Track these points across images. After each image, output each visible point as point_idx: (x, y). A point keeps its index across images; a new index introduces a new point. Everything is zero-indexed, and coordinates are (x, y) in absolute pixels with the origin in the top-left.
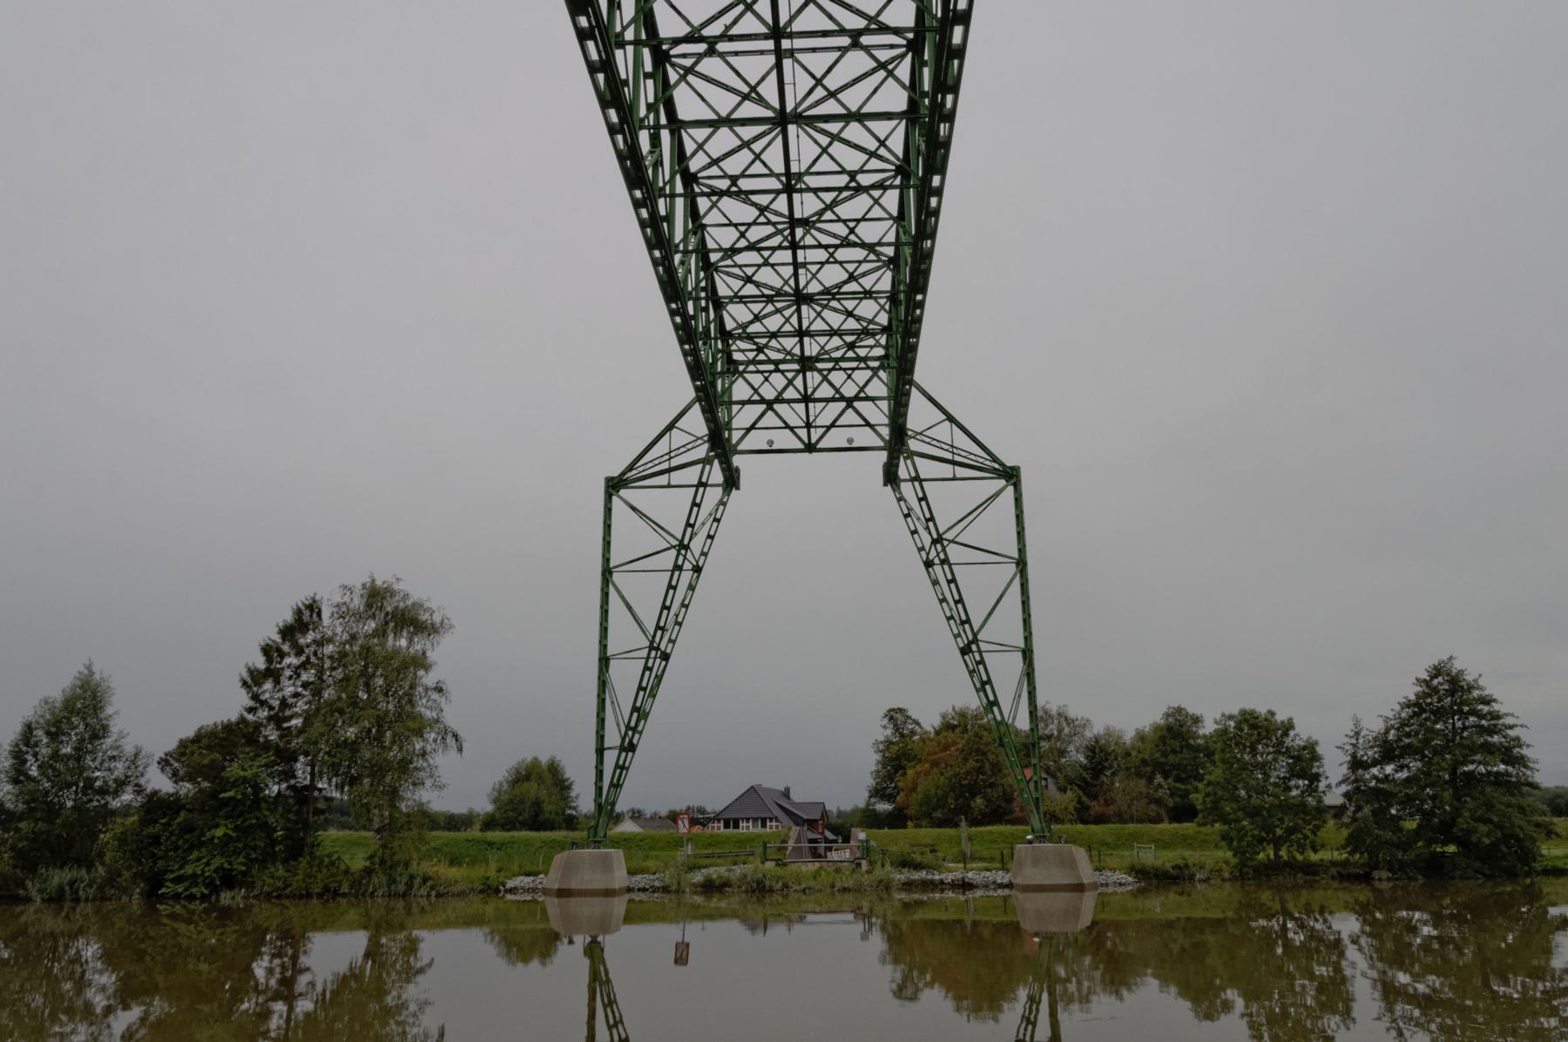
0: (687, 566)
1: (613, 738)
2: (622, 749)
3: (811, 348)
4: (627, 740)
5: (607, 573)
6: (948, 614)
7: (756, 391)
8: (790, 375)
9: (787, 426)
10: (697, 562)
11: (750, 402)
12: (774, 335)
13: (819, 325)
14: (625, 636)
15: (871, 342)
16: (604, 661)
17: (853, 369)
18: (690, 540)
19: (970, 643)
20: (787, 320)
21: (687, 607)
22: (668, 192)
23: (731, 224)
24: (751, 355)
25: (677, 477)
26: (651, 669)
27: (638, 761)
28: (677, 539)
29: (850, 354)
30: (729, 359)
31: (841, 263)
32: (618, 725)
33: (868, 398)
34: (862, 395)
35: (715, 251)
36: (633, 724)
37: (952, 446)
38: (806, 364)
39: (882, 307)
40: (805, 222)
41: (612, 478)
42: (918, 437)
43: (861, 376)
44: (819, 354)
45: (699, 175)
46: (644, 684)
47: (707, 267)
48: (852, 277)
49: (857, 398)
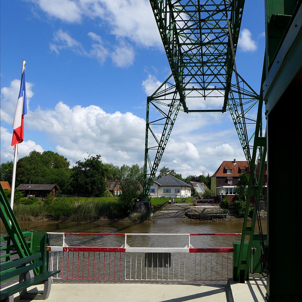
0: (170, 123)
2: (151, 174)
3: (205, 59)
4: (153, 172)
6: (240, 138)
7: (190, 71)
8: (199, 67)
9: (198, 82)
10: (172, 122)
11: (188, 75)
12: (195, 55)
13: (207, 52)
15: (222, 57)
17: (217, 66)
18: (170, 116)
19: (246, 146)
20: (199, 51)
21: (169, 135)
22: (165, 11)
23: (183, 20)
24: (188, 61)
26: (159, 152)
28: (167, 115)
29: (216, 61)
30: (182, 62)
31: (214, 33)
32: (150, 168)
33: (221, 75)
34: (219, 73)
35: (178, 29)
36: (154, 168)
37: (243, 89)
38: (203, 64)
39: (225, 47)
40: (204, 20)
41: (149, 97)
42: (234, 86)
43: (219, 68)
44: (207, 61)
45: (174, 5)
46: (157, 157)
47: (176, 34)
48: (217, 38)
49: (217, 74)
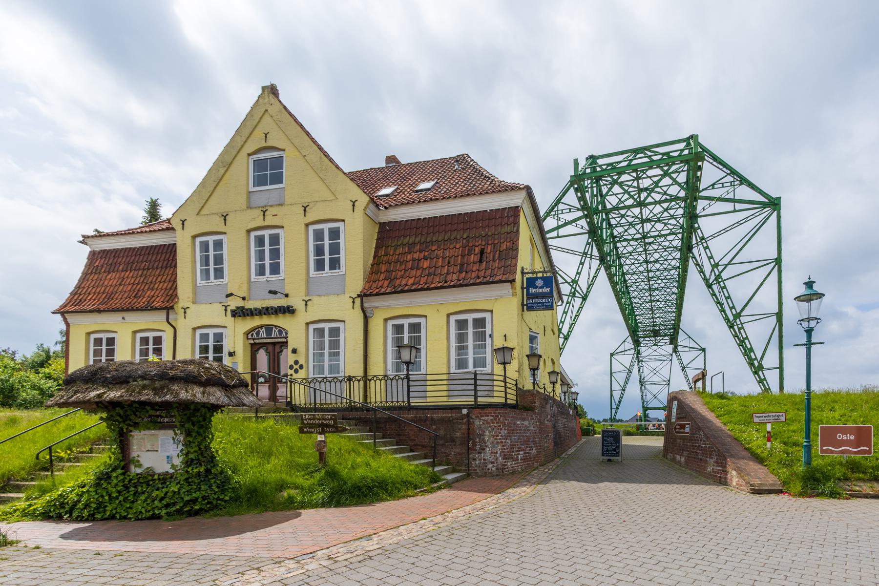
1: (614, 406)
5: (611, 374)
14: (616, 386)
16: (611, 392)
25: (626, 353)
27: (619, 411)
